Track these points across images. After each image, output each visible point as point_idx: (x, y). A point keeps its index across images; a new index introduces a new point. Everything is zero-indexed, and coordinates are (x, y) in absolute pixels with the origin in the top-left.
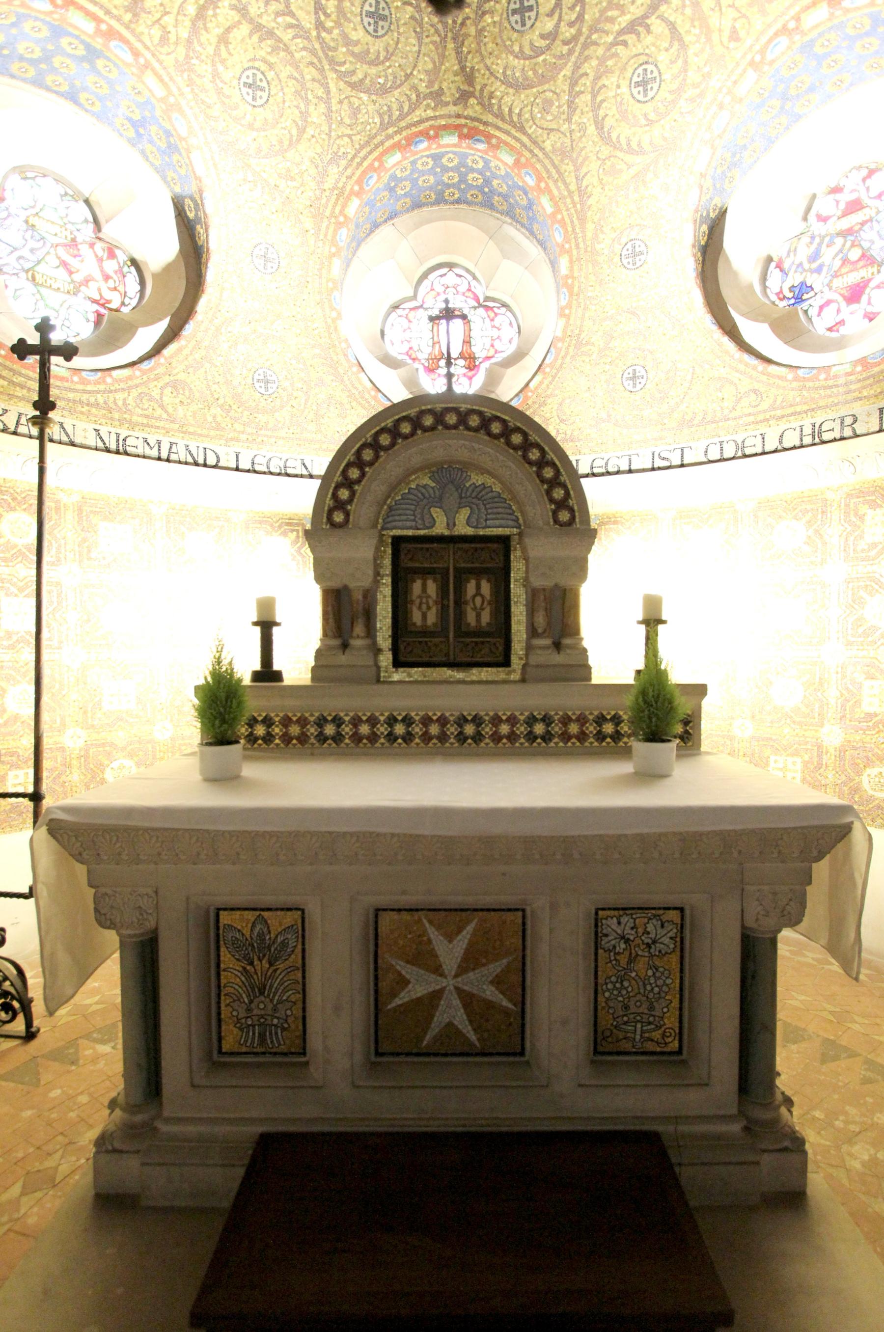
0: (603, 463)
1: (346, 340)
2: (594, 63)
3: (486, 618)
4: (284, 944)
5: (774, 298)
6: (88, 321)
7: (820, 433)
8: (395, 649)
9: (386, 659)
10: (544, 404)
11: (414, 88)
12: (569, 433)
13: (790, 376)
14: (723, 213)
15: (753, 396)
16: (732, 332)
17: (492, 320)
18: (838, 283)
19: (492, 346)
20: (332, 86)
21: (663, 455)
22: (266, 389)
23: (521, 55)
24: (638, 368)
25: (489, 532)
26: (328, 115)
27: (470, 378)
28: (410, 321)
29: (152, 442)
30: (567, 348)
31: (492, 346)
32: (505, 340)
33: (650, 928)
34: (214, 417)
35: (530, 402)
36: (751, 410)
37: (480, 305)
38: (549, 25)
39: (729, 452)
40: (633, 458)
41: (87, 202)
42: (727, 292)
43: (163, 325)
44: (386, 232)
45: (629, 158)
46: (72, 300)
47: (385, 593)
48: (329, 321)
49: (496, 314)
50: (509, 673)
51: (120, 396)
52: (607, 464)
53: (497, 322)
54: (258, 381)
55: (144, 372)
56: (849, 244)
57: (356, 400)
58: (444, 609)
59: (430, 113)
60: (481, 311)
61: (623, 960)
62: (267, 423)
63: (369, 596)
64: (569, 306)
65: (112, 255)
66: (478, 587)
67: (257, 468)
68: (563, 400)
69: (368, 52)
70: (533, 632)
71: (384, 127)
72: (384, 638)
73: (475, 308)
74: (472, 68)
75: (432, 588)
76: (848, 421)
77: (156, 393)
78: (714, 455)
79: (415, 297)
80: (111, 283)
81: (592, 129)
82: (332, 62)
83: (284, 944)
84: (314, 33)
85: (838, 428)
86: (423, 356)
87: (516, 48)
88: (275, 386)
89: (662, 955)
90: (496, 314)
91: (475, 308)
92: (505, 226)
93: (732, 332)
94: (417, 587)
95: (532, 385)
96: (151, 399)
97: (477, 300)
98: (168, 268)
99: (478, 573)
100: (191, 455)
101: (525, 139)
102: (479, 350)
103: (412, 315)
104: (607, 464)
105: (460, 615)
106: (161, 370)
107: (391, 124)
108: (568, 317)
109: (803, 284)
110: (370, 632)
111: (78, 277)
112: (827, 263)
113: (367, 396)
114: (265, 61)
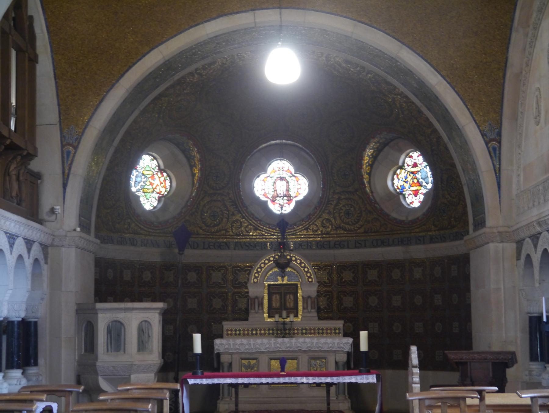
3: (292, 304)
4: (253, 366)
5: (396, 187)
6: (156, 200)
8: (269, 313)
9: (266, 315)
17: (297, 181)
19: (298, 192)
25: (292, 283)
27: (289, 204)
28: (265, 182)
31: (298, 192)
33: (320, 363)
37: (293, 176)
46: (153, 195)
47: (266, 297)
49: (299, 179)
50: (298, 319)
53: (300, 182)
56: (414, 177)
58: (281, 303)
60: (293, 178)
61: (315, 369)
63: (263, 298)
66: (290, 297)
70: (304, 308)
72: (266, 309)
73: (290, 177)
75: (278, 297)
80: (162, 185)
83: (253, 366)
86: (270, 196)
89: (322, 368)
90: (299, 179)
91: (290, 177)
94: (274, 297)
97: (292, 174)
99: (290, 293)
102: (292, 193)
103: (265, 180)
105: (285, 304)
112: (409, 181)
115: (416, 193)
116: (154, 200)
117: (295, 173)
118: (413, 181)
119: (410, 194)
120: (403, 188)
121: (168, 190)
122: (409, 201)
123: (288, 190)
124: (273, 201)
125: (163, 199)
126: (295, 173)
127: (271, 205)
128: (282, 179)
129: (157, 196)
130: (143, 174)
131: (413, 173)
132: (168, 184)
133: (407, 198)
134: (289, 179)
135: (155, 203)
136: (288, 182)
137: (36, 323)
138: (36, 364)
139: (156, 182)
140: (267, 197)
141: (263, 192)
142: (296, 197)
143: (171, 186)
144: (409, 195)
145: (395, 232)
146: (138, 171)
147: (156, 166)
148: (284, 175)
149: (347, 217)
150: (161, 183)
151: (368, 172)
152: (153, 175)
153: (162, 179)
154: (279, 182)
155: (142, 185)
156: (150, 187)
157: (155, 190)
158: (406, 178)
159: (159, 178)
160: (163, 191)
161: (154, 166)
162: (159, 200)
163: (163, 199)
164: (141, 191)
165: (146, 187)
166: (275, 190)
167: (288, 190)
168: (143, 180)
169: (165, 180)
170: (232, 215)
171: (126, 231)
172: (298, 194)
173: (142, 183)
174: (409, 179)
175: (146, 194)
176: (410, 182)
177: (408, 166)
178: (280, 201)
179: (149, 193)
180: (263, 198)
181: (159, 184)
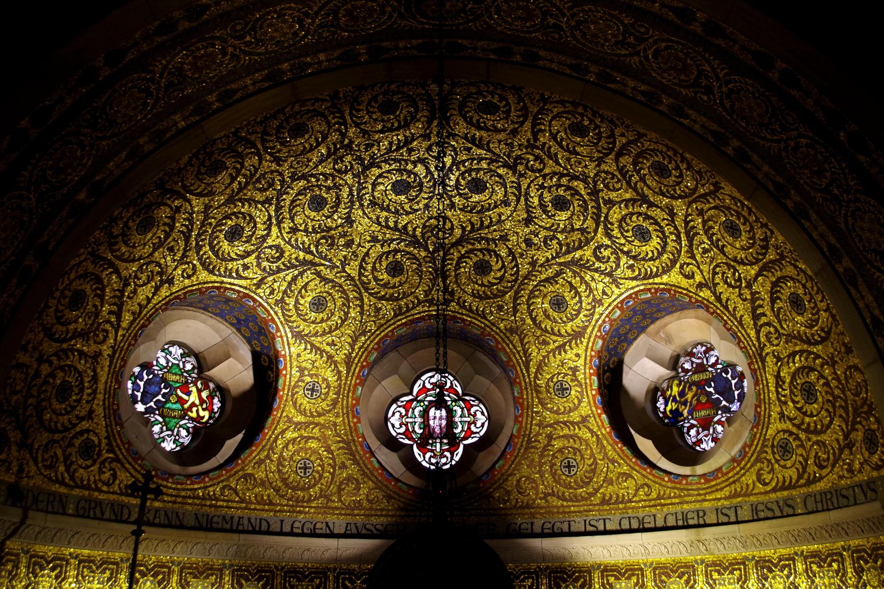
0: (550, 526)
1: (363, 436)
2: (527, 292)
7: (687, 519)
10: (506, 480)
11: (417, 297)
12: (525, 501)
13: (666, 479)
14: (620, 364)
15: (646, 489)
18: (697, 414)
20: (366, 300)
21: (592, 523)
22: (305, 474)
23: (482, 285)
24: (571, 460)
26: (362, 313)
29: (228, 518)
30: (522, 443)
32: (479, 424)
34: (269, 496)
35: (496, 479)
36: (645, 498)
38: (499, 274)
39: (635, 525)
40: (572, 523)
41: (196, 356)
43: (240, 436)
44: (393, 355)
45: (555, 338)
48: (352, 424)
51: (211, 489)
52: (553, 526)
53: (473, 410)
54: (300, 468)
55: (228, 471)
57: (367, 476)
59: (426, 309)
62: (304, 497)
64: (522, 415)
65: (206, 387)
67: (296, 531)
68: (521, 478)
69: (389, 283)
71: (396, 316)
73: (455, 401)
74: (453, 289)
76: (701, 514)
77: (233, 485)
78: (625, 525)
79: (411, 393)
81: (529, 321)
82: (366, 289)
84: (357, 278)
85: (696, 518)
87: (480, 282)
88: (311, 471)
92: (477, 352)
95: (497, 466)
96: (231, 488)
98: (246, 395)
100: (252, 525)
101: (487, 322)
104: (553, 526)
106: (239, 468)
107: (401, 314)
108: (521, 422)
109: (677, 409)
111: (186, 406)
113: (376, 474)
114: (327, 292)
115: (706, 424)
116: (184, 433)
117: (464, 394)
118: (698, 400)
119: (692, 426)
120: (676, 413)
121: (217, 415)
122: (691, 440)
123: (451, 424)
124: (422, 447)
125: (203, 431)
126: (464, 394)
127: (416, 450)
130: (164, 380)
131: (694, 383)
132: (217, 404)
133: (686, 435)
135: (185, 438)
139: (194, 398)
140: (411, 439)
141: (403, 430)
142: (465, 438)
143: (221, 409)
144: (689, 428)
145: (669, 501)
146: (153, 373)
147: (193, 368)
149: (567, 473)
150: (202, 401)
151: (607, 383)
152: (187, 383)
153: (204, 395)
155: (158, 401)
156: (178, 406)
157: (189, 413)
158: (682, 394)
159: (199, 391)
160: (206, 414)
161: (189, 367)
162: (195, 433)
163: (203, 431)
164: (157, 412)
165: (168, 406)
166: (426, 425)
168: (164, 391)
169: (211, 397)
170: (340, 468)
171: (105, 488)
172: (469, 433)
173: (160, 397)
174: (689, 396)
175: (167, 419)
176: (691, 402)
177: (686, 371)
179: (174, 417)
181: (197, 402)
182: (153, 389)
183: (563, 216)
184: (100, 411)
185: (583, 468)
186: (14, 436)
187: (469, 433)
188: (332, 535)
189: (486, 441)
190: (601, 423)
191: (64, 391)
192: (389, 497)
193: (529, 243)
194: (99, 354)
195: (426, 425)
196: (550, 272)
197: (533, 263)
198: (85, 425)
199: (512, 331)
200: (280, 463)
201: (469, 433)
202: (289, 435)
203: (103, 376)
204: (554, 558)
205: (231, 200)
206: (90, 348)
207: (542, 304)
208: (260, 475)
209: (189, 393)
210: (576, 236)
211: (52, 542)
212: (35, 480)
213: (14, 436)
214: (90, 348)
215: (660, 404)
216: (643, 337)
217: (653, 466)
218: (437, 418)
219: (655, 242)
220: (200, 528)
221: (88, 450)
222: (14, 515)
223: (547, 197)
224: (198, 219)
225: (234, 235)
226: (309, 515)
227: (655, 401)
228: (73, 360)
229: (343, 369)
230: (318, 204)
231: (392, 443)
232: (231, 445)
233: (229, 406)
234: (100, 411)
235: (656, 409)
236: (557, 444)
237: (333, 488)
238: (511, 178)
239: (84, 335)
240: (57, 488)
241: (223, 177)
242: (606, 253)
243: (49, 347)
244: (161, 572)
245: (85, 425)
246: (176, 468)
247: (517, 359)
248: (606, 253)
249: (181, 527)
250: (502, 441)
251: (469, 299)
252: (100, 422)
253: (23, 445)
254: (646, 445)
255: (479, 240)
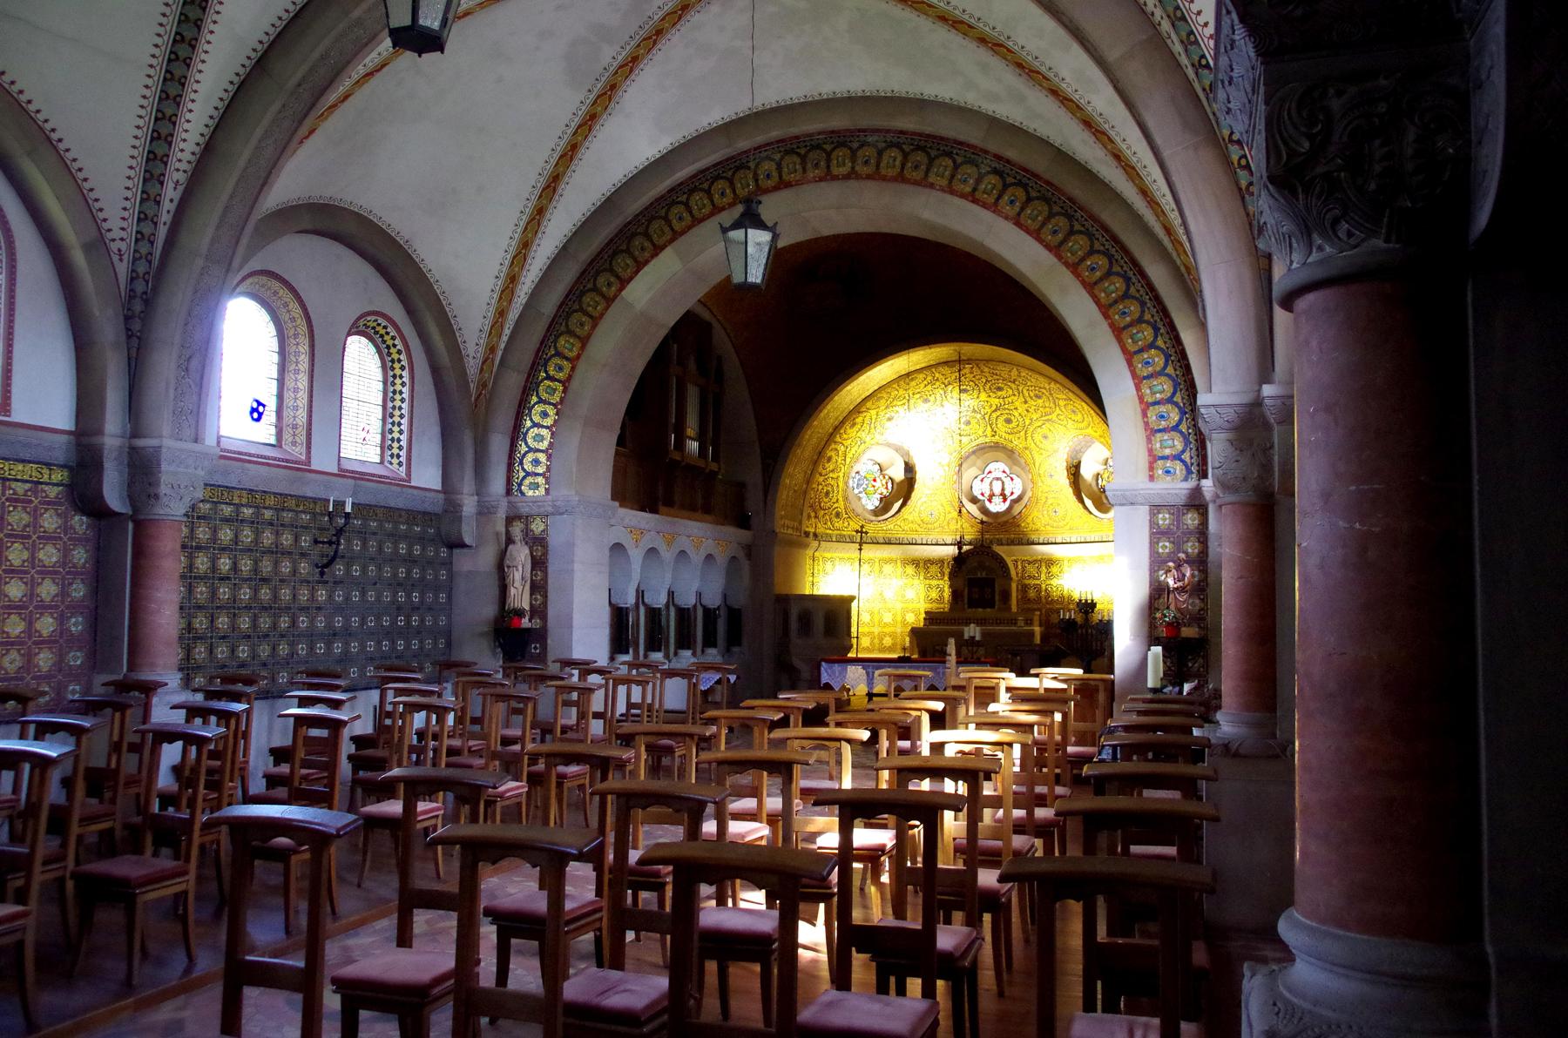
14: (1080, 462)
16: (1082, 502)
42: (1081, 487)
43: (900, 502)
47: (966, 591)
93: (1082, 502)
98: (902, 482)
102: (1007, 493)
110: (963, 601)
123: (1003, 489)
124: (990, 501)
127: (987, 503)
128: (998, 479)
129: (879, 496)
132: (890, 485)
134: (1004, 479)
135: (877, 503)
136: (1003, 483)
137: (739, 610)
138: (740, 644)
139: (878, 484)
148: (1003, 476)
153: (884, 482)
154: (995, 482)
160: (885, 492)
166: (991, 490)
167: (1003, 489)
173: (864, 486)
178: (996, 500)
180: (980, 497)
182: (861, 482)
183: (1040, 401)
184: (841, 499)
185: (1061, 512)
186: (813, 514)
187: (1012, 493)
188: (946, 544)
189: (1019, 499)
190: (1069, 492)
191: (827, 494)
192: (972, 526)
193: (1028, 411)
194: (838, 477)
195: (991, 490)
196: (1039, 424)
197: (1031, 419)
198: (836, 505)
199: (1026, 448)
200: (919, 513)
201: (1012, 493)
202: (923, 500)
203: (841, 485)
204: (1047, 554)
205: (887, 407)
206: (835, 476)
207: (1038, 437)
208: (911, 518)
209: (875, 480)
210: (1047, 409)
211: (829, 551)
212: (821, 530)
213: (813, 514)
214: (835, 476)
215: (1100, 481)
216: (1090, 449)
217: (1090, 513)
218: (997, 489)
219: (1080, 416)
220: (886, 543)
221: (838, 515)
222: (815, 544)
223: (1032, 394)
224: (875, 417)
225: (890, 419)
226: (932, 538)
227: (1097, 480)
228: (830, 481)
229: (947, 468)
230: (926, 401)
231: (974, 500)
232: (897, 505)
233: (895, 487)
234: (841, 499)
235: (1097, 484)
236: (1050, 501)
237: (945, 523)
238: (1013, 386)
239: (833, 471)
240: (828, 531)
241: (883, 401)
242: (1062, 417)
243: (821, 479)
244: (871, 561)
245: (836, 505)
246: (874, 518)
247: (1030, 461)
248: (1062, 417)
249: (878, 543)
250: (1026, 499)
251: (1004, 434)
252: (841, 504)
253: (816, 517)
254: (1088, 503)
255: (1005, 409)
